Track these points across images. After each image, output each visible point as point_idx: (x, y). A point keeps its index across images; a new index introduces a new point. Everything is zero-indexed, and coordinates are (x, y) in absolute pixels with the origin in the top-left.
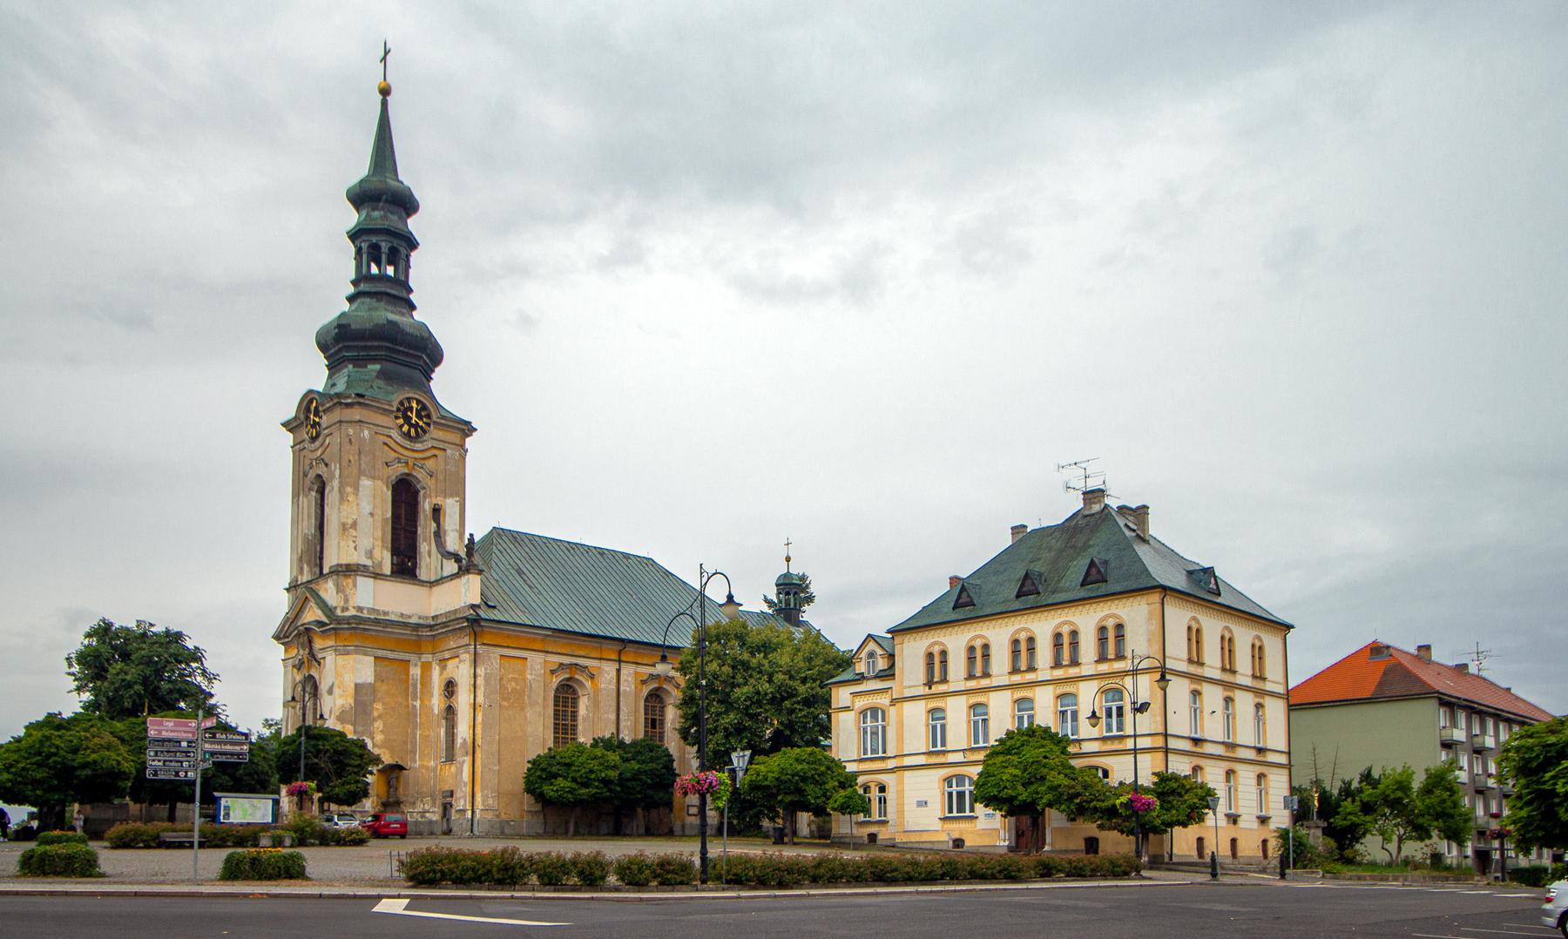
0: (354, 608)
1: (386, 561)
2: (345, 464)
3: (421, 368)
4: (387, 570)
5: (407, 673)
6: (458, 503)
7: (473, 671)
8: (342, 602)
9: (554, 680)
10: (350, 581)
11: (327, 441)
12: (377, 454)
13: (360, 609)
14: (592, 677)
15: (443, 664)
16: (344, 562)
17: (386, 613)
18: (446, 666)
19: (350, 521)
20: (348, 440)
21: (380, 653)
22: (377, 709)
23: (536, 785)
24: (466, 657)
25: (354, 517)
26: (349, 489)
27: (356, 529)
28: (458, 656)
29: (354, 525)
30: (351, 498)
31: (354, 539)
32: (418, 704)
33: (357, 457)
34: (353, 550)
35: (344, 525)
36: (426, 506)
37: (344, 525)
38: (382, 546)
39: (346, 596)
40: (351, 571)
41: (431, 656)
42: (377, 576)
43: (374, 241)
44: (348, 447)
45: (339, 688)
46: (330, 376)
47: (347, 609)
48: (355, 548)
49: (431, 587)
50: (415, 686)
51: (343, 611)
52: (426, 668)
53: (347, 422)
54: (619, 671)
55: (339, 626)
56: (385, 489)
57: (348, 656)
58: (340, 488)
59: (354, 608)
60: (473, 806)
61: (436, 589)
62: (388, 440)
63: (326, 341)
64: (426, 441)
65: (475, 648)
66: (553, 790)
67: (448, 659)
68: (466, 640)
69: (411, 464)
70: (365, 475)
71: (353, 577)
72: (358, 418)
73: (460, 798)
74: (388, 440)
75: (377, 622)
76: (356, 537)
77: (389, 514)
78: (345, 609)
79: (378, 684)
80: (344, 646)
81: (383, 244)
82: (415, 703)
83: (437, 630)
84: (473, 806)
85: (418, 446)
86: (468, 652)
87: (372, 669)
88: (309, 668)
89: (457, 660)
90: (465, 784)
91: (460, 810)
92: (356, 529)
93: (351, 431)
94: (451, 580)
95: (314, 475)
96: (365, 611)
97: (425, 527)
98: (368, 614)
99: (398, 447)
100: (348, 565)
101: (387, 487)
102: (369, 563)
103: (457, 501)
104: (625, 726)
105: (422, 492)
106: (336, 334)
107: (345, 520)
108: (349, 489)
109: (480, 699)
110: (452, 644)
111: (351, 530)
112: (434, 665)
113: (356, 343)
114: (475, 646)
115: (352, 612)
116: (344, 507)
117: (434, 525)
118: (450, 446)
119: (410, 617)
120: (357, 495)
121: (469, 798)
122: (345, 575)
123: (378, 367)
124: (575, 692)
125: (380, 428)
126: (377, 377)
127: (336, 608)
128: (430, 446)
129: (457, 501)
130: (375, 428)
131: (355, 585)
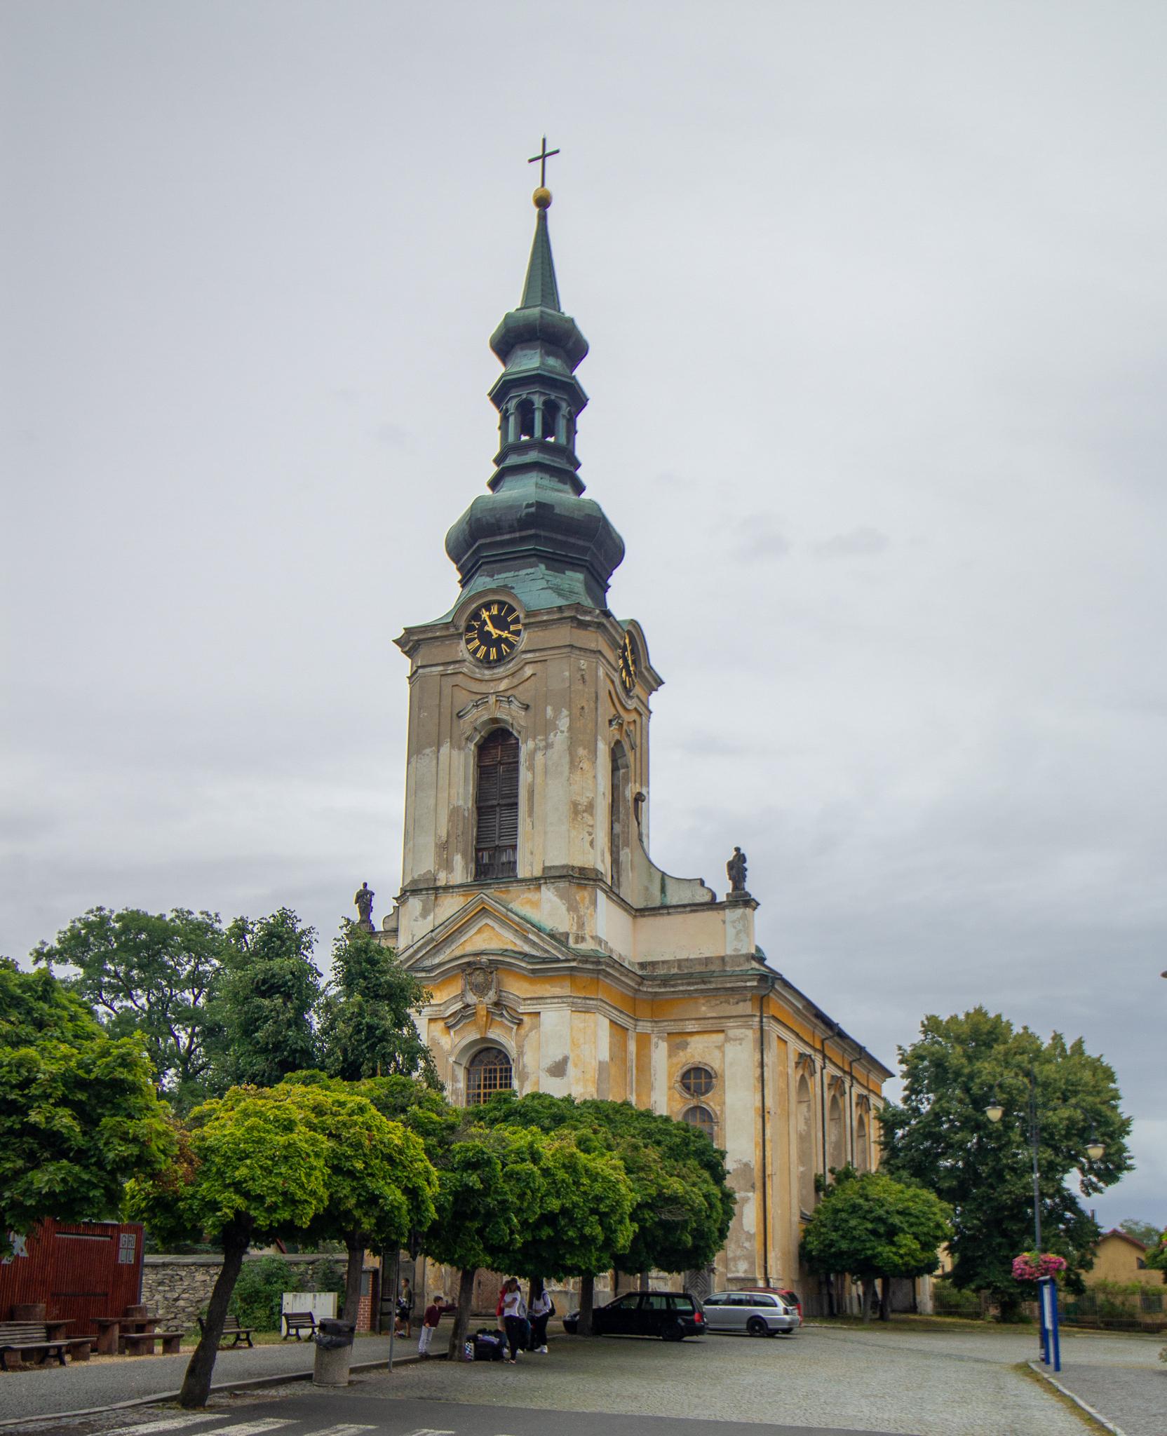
0: (592, 937)
2: (576, 711)
7: (758, 1056)
8: (575, 928)
10: (586, 894)
11: (528, 671)
13: (599, 941)
16: (577, 863)
18: (684, 1046)
19: (584, 801)
20: (579, 676)
23: (868, 1245)
24: (750, 1035)
25: (591, 795)
26: (581, 752)
27: (592, 815)
28: (723, 1031)
29: (590, 808)
30: (586, 765)
33: (592, 705)
34: (587, 845)
35: (575, 805)
37: (575, 805)
40: (588, 879)
41: (649, 1024)
43: (553, 397)
44: (581, 687)
45: (576, 1065)
47: (583, 939)
48: (592, 843)
49: (635, 917)
51: (577, 942)
52: (643, 1041)
53: (580, 649)
55: (581, 965)
57: (588, 1015)
58: (569, 748)
59: (592, 937)
60: (766, 1273)
61: (648, 922)
65: (761, 1022)
66: (895, 1254)
67: (692, 1034)
68: (746, 1008)
71: (589, 889)
72: (593, 646)
73: (735, 1259)
76: (592, 826)
78: (580, 939)
80: (585, 998)
81: (564, 405)
83: (673, 986)
84: (766, 1273)
86: (749, 1027)
88: (489, 1024)
89: (721, 1037)
90: (750, 1237)
92: (592, 815)
93: (583, 664)
94: (692, 911)
95: (485, 717)
100: (582, 869)
105: (622, 771)
106: (527, 514)
107: (578, 798)
108: (581, 752)
109: (769, 1103)
110: (704, 1010)
111: (585, 815)
112: (654, 1040)
113: (554, 536)
114: (761, 1017)
115: (588, 946)
116: (577, 777)
120: (594, 762)
121: (759, 1261)
122: (579, 884)
127: (567, 935)
131: (594, 903)
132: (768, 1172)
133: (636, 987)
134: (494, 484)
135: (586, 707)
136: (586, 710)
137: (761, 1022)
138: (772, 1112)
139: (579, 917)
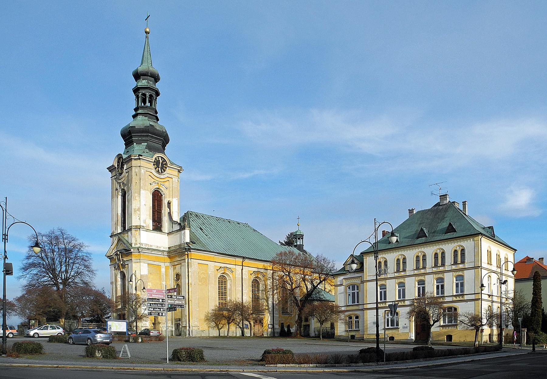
1: (150, 223)
3: (162, 144)
4: (151, 228)
5: (160, 271)
6: (177, 200)
8: (135, 241)
9: (218, 274)
12: (146, 180)
14: (232, 272)
15: (174, 267)
17: (151, 246)
19: (137, 208)
21: (151, 262)
22: (150, 285)
31: (139, 215)
32: (164, 283)
36: (165, 202)
38: (149, 218)
39: (136, 239)
42: (148, 230)
43: (144, 92)
46: (126, 148)
50: (163, 275)
54: (242, 270)
56: (150, 194)
62: (151, 174)
63: (125, 133)
64: (164, 174)
69: (159, 184)
70: (143, 189)
74: (151, 174)
75: (148, 249)
77: (151, 205)
79: (149, 275)
81: (147, 93)
82: (163, 283)
85: (162, 176)
87: (147, 269)
91: (184, 326)
94: (177, 232)
96: (144, 245)
97: (165, 211)
98: (145, 246)
99: (155, 177)
101: (151, 193)
102: (144, 225)
103: (177, 200)
104: (245, 292)
111: (137, 211)
117: (169, 209)
118: (174, 176)
119: (160, 248)
123: (146, 144)
124: (225, 278)
125: (148, 169)
126: (146, 148)
128: (166, 177)
129: (177, 200)
130: (146, 169)
132: (190, 300)
133: (163, 254)
134: (134, 116)
135: (137, 182)
136: (137, 183)
137: (188, 260)
138: (193, 284)
139: (136, 239)
